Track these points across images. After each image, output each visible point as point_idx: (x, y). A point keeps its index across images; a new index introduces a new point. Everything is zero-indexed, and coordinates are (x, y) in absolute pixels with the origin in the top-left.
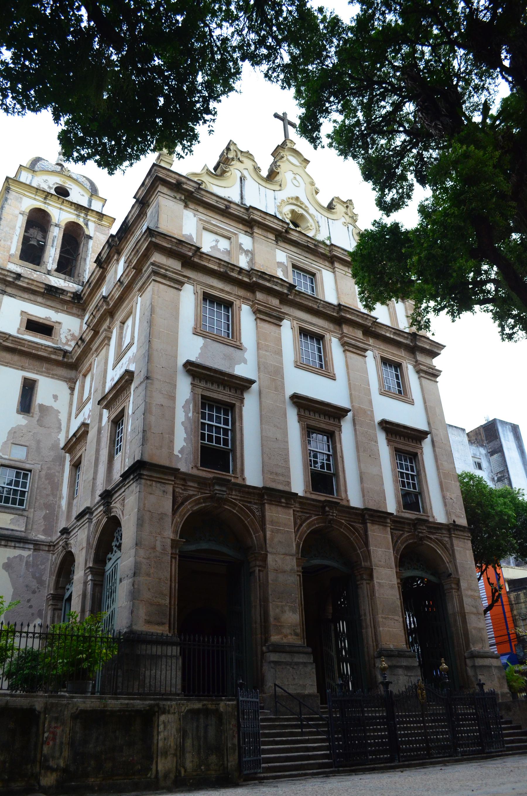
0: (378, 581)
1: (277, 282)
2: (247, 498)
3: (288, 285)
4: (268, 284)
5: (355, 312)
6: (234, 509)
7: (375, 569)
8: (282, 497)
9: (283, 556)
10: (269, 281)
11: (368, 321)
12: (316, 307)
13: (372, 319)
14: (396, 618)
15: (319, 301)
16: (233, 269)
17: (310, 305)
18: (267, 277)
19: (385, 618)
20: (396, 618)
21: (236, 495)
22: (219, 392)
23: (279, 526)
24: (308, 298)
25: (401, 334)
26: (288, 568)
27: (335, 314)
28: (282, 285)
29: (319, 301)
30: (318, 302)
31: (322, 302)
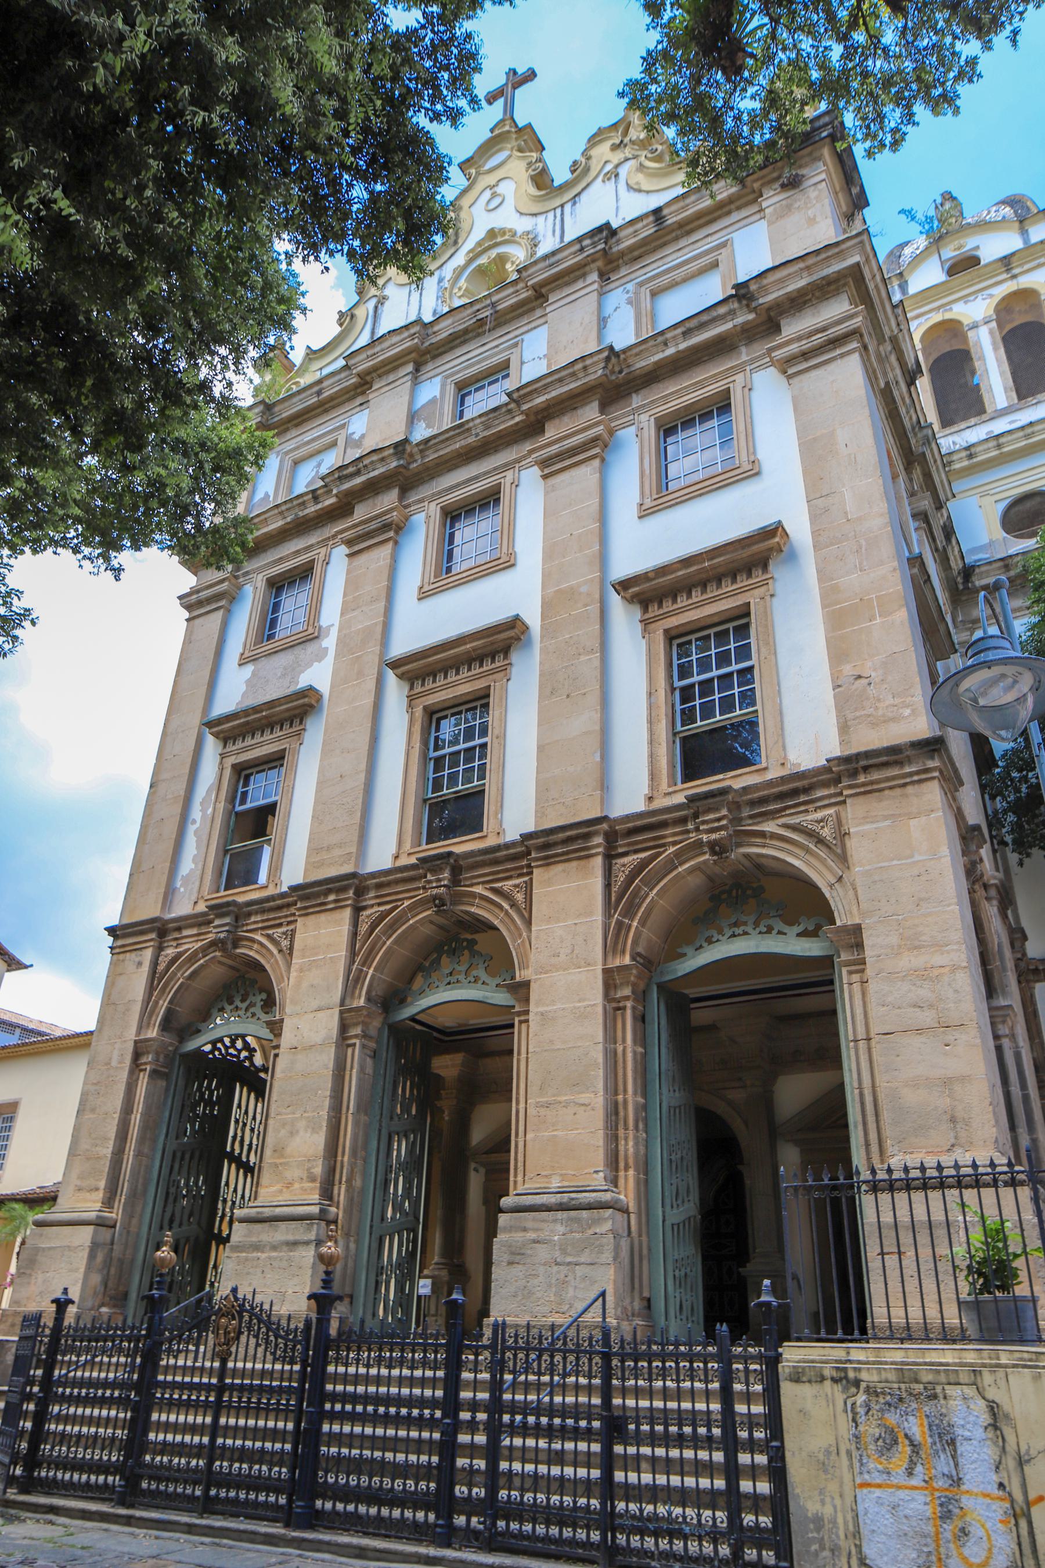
0: (541, 1009)
1: (372, 462)
2: (275, 919)
3: (391, 451)
4: (359, 480)
5: (549, 380)
6: (251, 949)
7: (536, 980)
8: (329, 891)
9: (312, 1015)
10: (358, 473)
11: (591, 371)
12: (471, 440)
13: (595, 359)
14: (584, 1098)
15: (471, 424)
16: (303, 503)
17: (458, 446)
18: (351, 470)
19: (547, 1106)
20: (584, 1098)
21: (255, 922)
22: (260, 745)
23: (317, 954)
24: (447, 439)
25: (705, 318)
26: (317, 1038)
27: (517, 419)
28: (383, 459)
29: (471, 424)
30: (469, 429)
31: (478, 421)
